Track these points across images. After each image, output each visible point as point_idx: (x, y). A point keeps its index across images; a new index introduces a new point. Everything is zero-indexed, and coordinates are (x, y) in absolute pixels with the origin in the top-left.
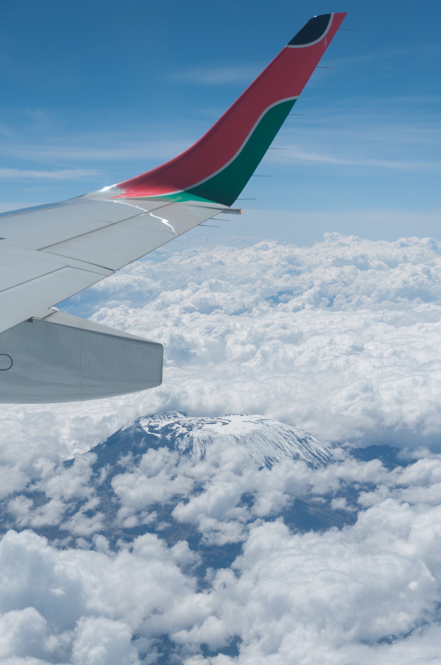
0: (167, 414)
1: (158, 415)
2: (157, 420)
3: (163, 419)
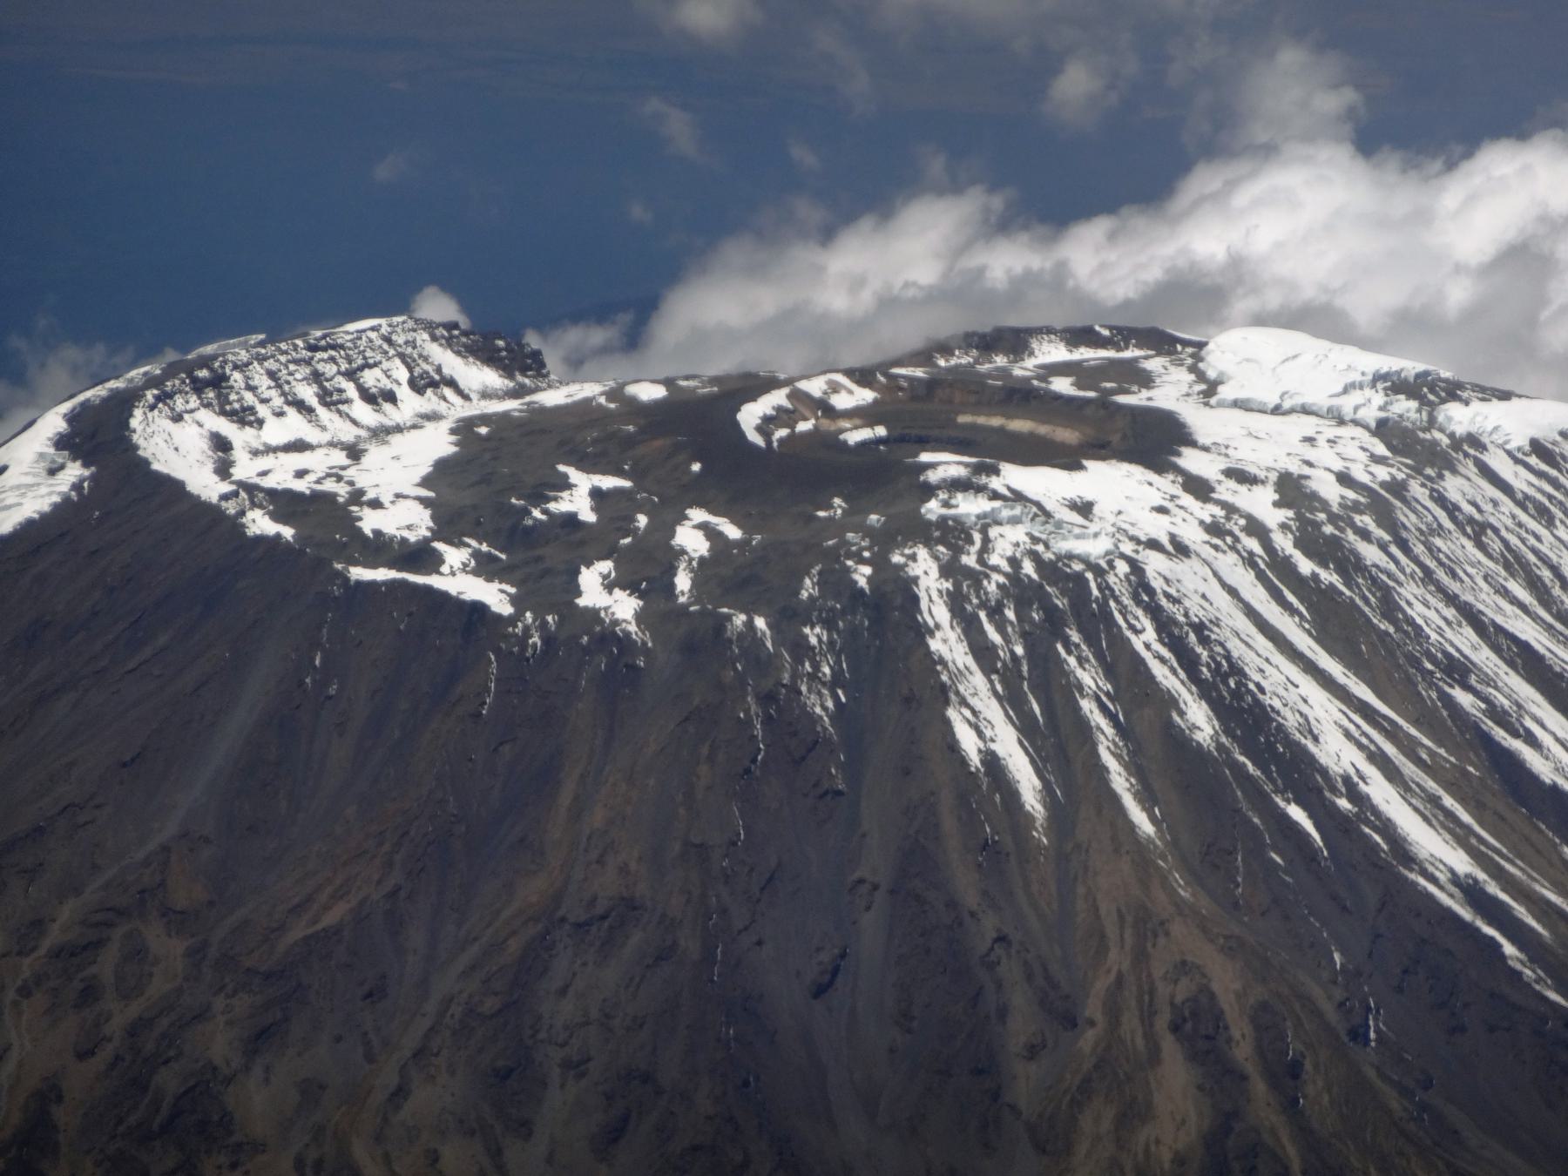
0: (349, 360)
1: (272, 375)
2: (277, 431)
3: (322, 412)
